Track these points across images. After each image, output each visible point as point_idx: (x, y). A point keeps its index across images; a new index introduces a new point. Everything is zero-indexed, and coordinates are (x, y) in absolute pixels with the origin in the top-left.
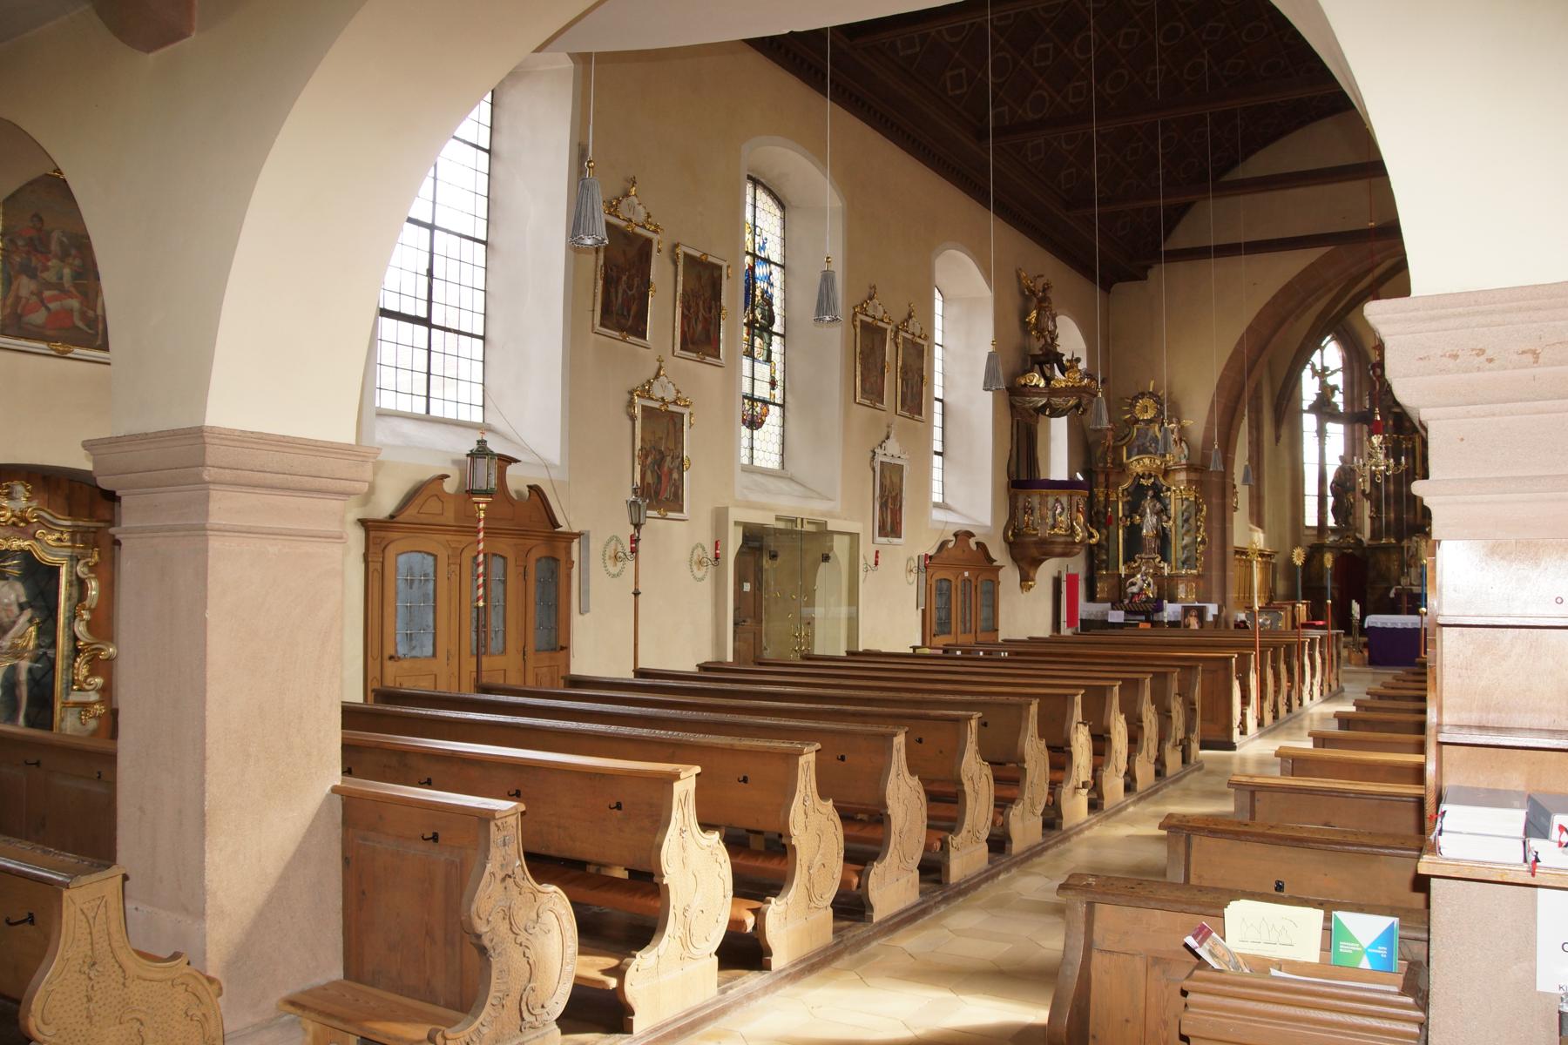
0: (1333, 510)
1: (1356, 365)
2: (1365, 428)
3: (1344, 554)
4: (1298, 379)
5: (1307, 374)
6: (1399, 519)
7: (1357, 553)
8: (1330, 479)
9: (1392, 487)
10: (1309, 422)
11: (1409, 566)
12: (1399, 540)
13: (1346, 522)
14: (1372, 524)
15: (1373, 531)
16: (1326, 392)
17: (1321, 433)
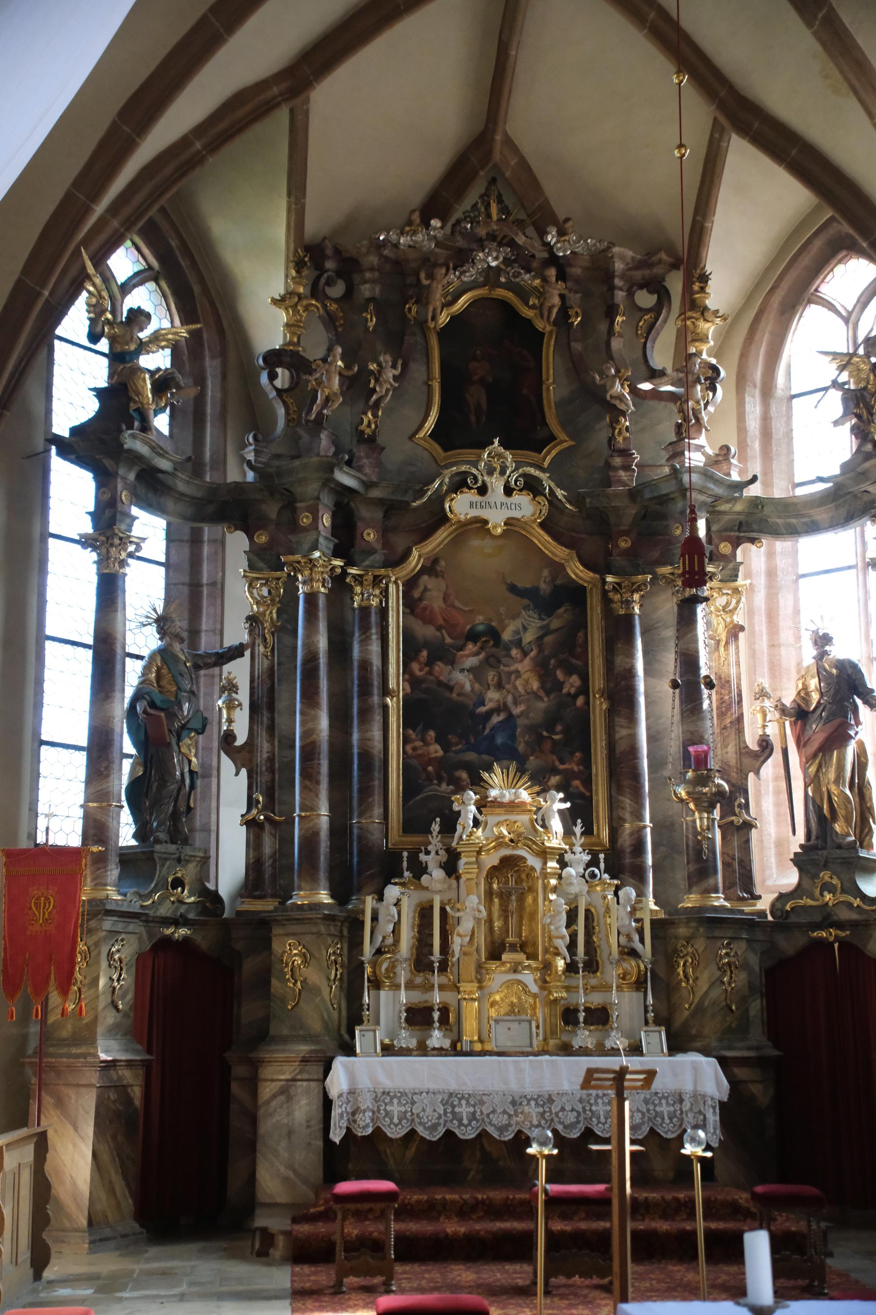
0: (137, 792)
1: (211, 366)
2: (237, 543)
3: (165, 943)
4: (43, 339)
5: (75, 322)
6: (340, 829)
7: (204, 941)
8: (133, 674)
9: (324, 723)
10: (71, 492)
11: (376, 984)
12: (341, 894)
13: (178, 836)
14: (254, 845)
15: (254, 867)
16: (119, 398)
17: (107, 533)
